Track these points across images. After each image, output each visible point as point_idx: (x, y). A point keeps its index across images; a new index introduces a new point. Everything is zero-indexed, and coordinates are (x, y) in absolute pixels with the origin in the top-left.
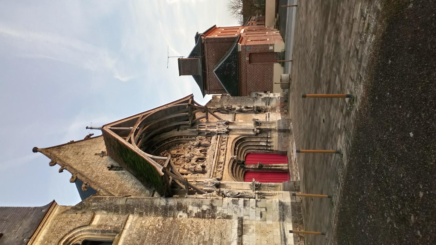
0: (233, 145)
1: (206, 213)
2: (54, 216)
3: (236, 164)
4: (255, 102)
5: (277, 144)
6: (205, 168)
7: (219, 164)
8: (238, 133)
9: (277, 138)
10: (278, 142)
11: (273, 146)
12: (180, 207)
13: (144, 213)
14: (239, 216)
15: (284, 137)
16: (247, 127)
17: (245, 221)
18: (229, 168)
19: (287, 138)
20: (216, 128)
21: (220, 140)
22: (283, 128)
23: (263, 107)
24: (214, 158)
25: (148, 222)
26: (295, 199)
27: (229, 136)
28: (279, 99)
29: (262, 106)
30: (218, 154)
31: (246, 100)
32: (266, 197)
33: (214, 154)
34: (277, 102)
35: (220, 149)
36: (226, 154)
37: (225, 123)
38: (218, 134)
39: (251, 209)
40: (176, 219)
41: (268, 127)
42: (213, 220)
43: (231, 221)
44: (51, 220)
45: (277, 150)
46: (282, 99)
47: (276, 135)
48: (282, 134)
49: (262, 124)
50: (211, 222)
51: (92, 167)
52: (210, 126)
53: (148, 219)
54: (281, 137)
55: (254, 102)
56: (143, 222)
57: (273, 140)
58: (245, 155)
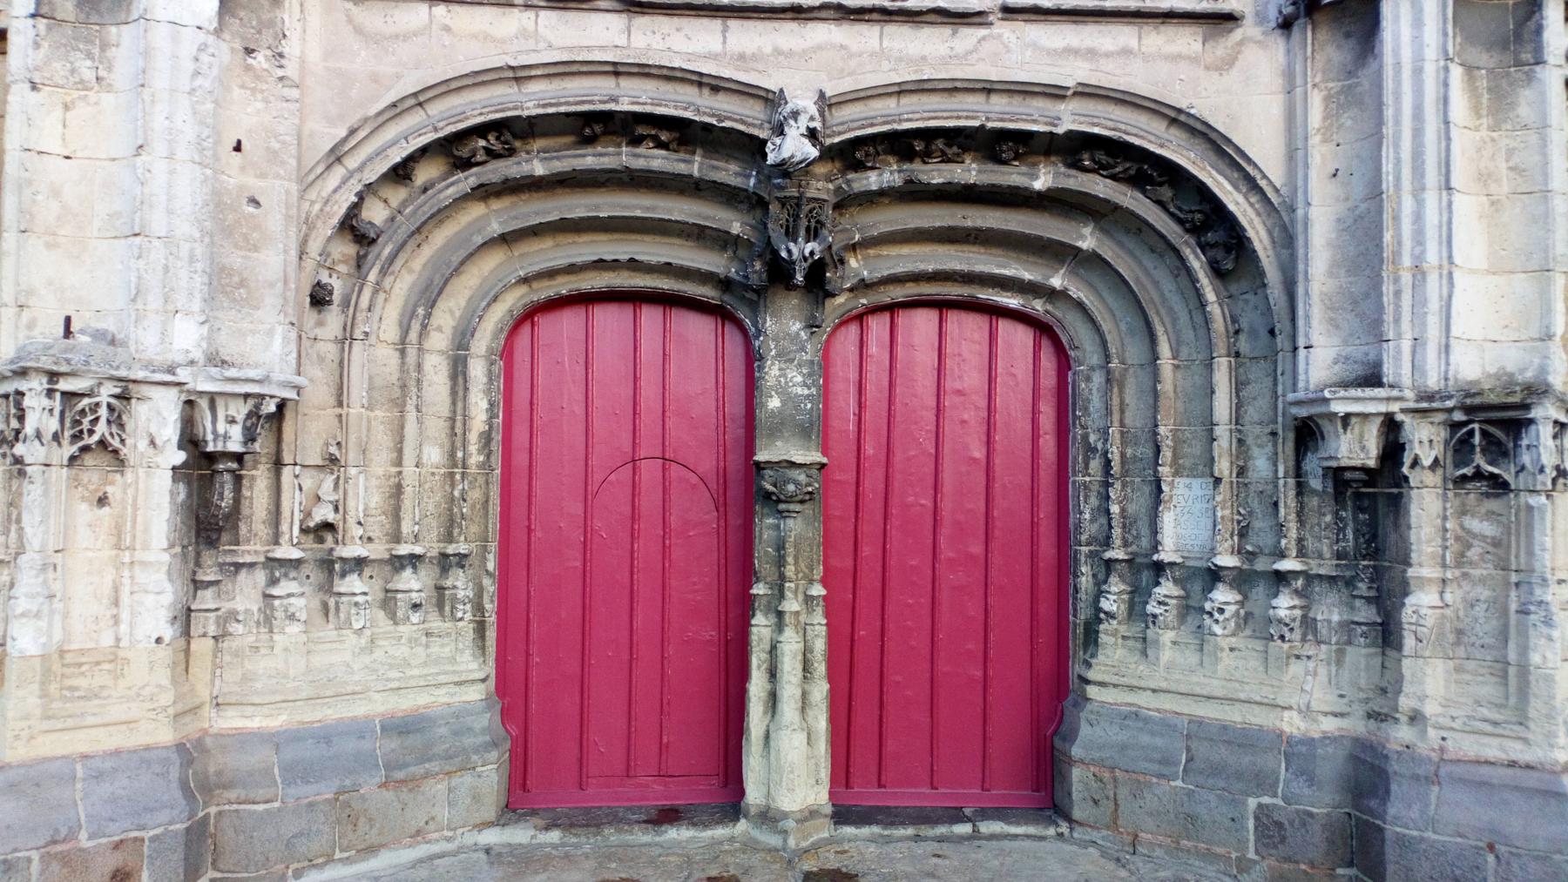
3: (729, 172)
5: (1168, 703)
8: (1320, 157)
9: (1260, 718)
11: (1145, 646)
15: (1271, 830)
16: (1419, 271)
18: (605, 85)
22: (1403, 842)
45: (1092, 691)
47: (1306, 712)
49: (1493, 505)
54: (1265, 782)
57: (1227, 660)
58: (1012, 301)
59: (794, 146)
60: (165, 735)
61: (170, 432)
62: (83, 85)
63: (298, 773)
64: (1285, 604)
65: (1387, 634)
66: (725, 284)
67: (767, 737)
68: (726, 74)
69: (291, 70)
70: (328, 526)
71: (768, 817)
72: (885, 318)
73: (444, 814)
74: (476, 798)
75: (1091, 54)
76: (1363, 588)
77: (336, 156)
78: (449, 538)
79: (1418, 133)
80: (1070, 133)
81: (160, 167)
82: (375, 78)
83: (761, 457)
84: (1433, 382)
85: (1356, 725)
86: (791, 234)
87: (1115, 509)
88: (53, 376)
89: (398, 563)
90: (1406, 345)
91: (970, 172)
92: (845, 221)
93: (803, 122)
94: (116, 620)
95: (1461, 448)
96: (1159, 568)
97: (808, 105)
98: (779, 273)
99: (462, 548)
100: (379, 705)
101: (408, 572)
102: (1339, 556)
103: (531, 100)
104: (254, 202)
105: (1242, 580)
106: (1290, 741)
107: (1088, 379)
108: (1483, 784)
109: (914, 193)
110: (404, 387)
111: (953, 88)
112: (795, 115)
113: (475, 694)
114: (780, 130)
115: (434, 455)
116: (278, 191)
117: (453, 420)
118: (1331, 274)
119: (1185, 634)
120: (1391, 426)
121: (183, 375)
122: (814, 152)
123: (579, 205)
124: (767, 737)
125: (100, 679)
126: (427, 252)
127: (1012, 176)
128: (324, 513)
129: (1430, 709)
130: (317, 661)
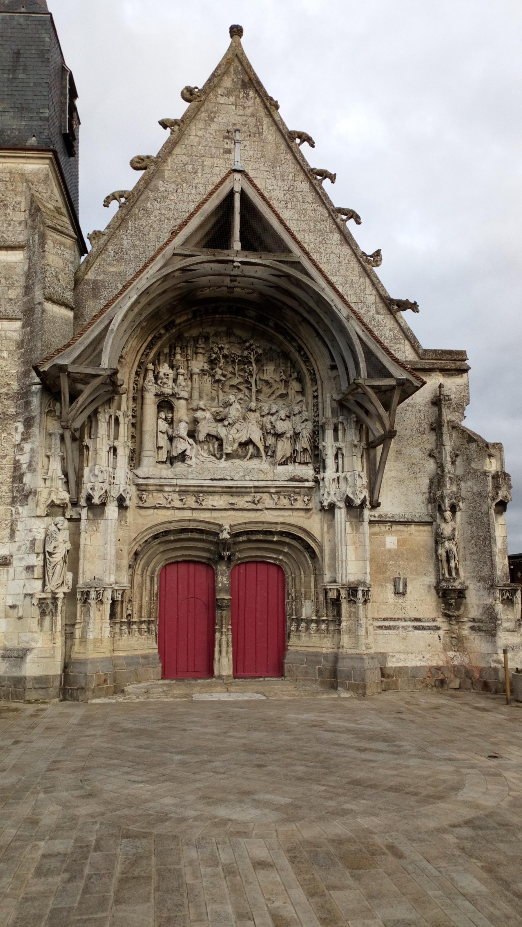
0: (279, 526)
1: (20, 483)
2: (20, 166)
3: (211, 538)
4: (478, 584)
5: (303, 649)
6: (179, 463)
7: (196, 494)
8: (326, 536)
9: (319, 650)
10: (309, 654)
11: (299, 637)
12: (28, 423)
13: (23, 350)
14: (14, 557)
15: (320, 672)
16: (342, 562)
17: (5, 571)
18: (188, 523)
19: (316, 680)
20: (337, 471)
21: (297, 490)
22: (340, 670)
23: (465, 610)
24: (212, 480)
25: (4, 364)
26: (36, 686)
27: (314, 511)
28: (493, 665)
29: (470, 606)
30: (234, 490)
31: (483, 553)
32: (48, 619)
33: (226, 480)
34: (484, 656)
35: (255, 492)
36: (233, 509)
37: (347, 496)
38: (316, 481)
39: (22, 582)
40: (12, 422)
41: (344, 624)
42: (9, 500)
43: (7, 540)
44: (13, 165)
45: (289, 648)
46: (493, 673)
47: (327, 648)
48: (328, 666)
49: (354, 605)
50: (4, 496)
51: (179, 191)
52: (343, 455)
53: (13, 362)
54: (319, 663)
55: (479, 581)
56: (5, 354)
57: (314, 638)
58: (272, 561)
59: (225, 535)
60: (108, 655)
61: (110, 597)
62: (94, 531)
63: (128, 664)
64: (323, 626)
65: (339, 631)
66: (209, 559)
67: (219, 660)
68: (211, 521)
69: (128, 524)
70: (129, 615)
71: (220, 677)
72: (244, 566)
73: (152, 676)
74: (158, 674)
75: (283, 516)
76: (337, 622)
77: (135, 539)
78: (150, 617)
79: (341, 535)
80: (280, 531)
81: (109, 547)
82: (143, 524)
83: (218, 597)
84: (345, 582)
85: (335, 650)
86: (224, 550)
87: (294, 607)
88: (95, 588)
89: (141, 622)
90: (340, 575)
91: (261, 537)
92: (235, 547)
93: (227, 531)
94: (101, 633)
95: (349, 595)
96: (302, 620)
97: (227, 527)
98: (221, 558)
99: (153, 619)
100: (139, 652)
101: (143, 625)
102: (333, 616)
103: (172, 527)
104: (121, 550)
105: (318, 622)
106: (324, 654)
107: (288, 578)
108: (352, 658)
109: (249, 541)
110: (142, 584)
111: (256, 523)
112: (225, 529)
113: (156, 651)
114: (222, 531)
115: (147, 599)
116: (125, 548)
117: (151, 591)
118: (329, 560)
119: (307, 634)
120: (338, 591)
121: (113, 586)
122: (229, 537)
123: (179, 545)
124: (219, 660)
125: (99, 644)
126: (147, 555)
127: (269, 538)
128: (129, 612)
129: (345, 645)
130: (129, 642)
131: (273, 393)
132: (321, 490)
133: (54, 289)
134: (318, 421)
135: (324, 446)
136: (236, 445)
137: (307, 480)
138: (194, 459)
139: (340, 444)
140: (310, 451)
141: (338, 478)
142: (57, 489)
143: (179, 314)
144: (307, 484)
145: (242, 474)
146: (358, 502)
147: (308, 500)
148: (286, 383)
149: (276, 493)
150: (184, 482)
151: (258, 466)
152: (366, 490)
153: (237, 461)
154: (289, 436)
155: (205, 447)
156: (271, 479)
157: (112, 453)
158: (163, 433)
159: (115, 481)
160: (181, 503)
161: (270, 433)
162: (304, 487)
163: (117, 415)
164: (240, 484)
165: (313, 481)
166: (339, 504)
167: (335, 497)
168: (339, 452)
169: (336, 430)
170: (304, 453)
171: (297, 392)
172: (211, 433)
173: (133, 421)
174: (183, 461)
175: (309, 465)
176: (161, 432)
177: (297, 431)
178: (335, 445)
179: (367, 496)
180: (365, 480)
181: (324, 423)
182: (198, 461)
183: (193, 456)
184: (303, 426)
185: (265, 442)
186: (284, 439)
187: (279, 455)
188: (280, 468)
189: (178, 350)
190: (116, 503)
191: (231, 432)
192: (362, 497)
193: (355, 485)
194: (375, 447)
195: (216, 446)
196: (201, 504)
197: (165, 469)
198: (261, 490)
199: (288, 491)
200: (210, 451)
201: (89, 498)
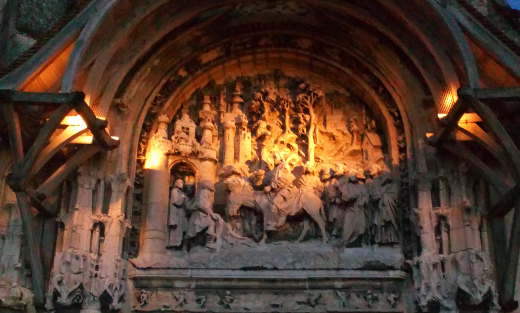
6: (198, 248)
7: (221, 291)
20: (441, 251)
21: (378, 284)
24: (244, 269)
30: (279, 284)
33: (266, 269)
35: (312, 288)
38: (407, 269)
52: (448, 226)
131: (340, 150)
132: (416, 283)
133: (33, 19)
134: (407, 184)
135: (416, 215)
136: (283, 219)
137: (392, 268)
138: (219, 242)
139: (443, 210)
140: (396, 225)
141: (443, 263)
142: (10, 284)
143: (205, 49)
144: (392, 274)
145: (290, 260)
146: (479, 298)
147: (395, 299)
148: (362, 138)
149: (344, 289)
150: (203, 274)
151: (315, 249)
152: (490, 281)
153: (285, 243)
154: (361, 203)
155: (239, 225)
156: (336, 267)
157: (97, 234)
158: (178, 207)
159: (98, 272)
160: (198, 305)
161: (335, 203)
162: (388, 279)
163: (108, 179)
164: (286, 275)
165: (402, 269)
166: (445, 303)
167: (439, 292)
168: (443, 223)
169: (435, 192)
170: (386, 230)
171: (375, 147)
172: (246, 205)
173: (139, 191)
174: (203, 245)
175: (395, 246)
176: (175, 205)
177: (375, 198)
178: (433, 212)
179: (493, 289)
180: (488, 265)
181: (416, 181)
182: (225, 244)
183: (218, 236)
184: (384, 189)
185: (327, 216)
186: (356, 209)
187: (348, 230)
188: (349, 252)
189: (207, 100)
190: (98, 305)
191: (275, 200)
192: (485, 290)
193: (471, 270)
194: (502, 214)
195: (254, 222)
196: (228, 307)
197: (178, 256)
198: (320, 284)
199: (364, 286)
200: (245, 231)
201: (57, 294)
